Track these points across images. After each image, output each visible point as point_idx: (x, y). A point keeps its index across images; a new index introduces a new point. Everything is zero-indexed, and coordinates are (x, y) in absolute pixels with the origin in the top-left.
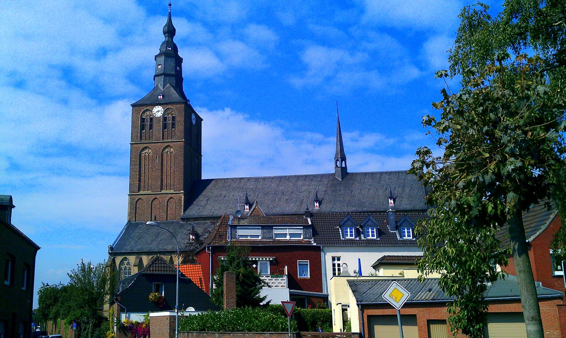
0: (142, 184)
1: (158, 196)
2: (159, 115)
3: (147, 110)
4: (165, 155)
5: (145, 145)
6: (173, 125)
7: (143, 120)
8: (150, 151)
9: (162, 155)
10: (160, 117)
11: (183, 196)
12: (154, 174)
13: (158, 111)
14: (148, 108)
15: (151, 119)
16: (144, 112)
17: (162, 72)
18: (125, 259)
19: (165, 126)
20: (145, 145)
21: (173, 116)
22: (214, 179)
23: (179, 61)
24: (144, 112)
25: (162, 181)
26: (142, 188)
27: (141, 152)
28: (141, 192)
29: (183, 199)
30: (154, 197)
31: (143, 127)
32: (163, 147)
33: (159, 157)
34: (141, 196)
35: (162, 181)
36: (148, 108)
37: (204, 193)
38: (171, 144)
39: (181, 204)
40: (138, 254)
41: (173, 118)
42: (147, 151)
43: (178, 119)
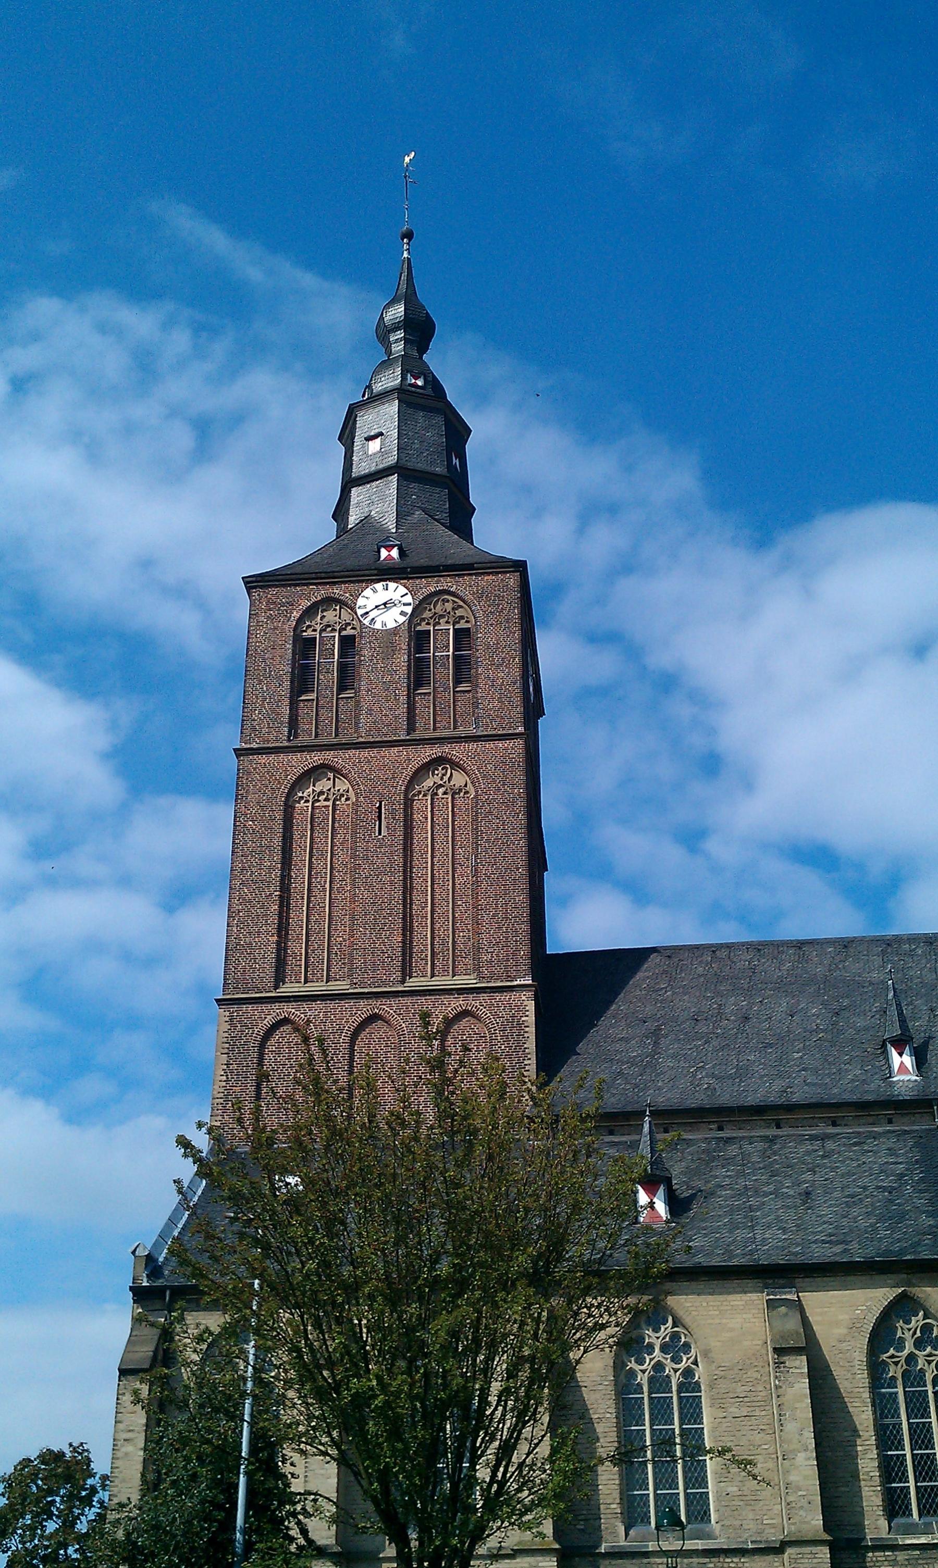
0: (297, 947)
1: (386, 1007)
2: (392, 619)
3: (329, 601)
4: (423, 805)
5: (316, 758)
6: (463, 668)
7: (304, 647)
8: (342, 785)
9: (408, 804)
10: (395, 631)
11: (531, 1006)
12: (363, 893)
13: (384, 606)
14: (337, 591)
15: (348, 643)
16: (310, 612)
17: (392, 459)
18: (655, 1315)
19: (419, 674)
20: (316, 758)
21: (462, 625)
22: (654, 950)
23: (457, 433)
24: (310, 612)
25: (407, 929)
26: (295, 964)
27: (289, 795)
28: (289, 988)
29: (531, 1019)
30: (365, 1008)
31: (302, 680)
32: (410, 770)
33: (393, 812)
34: (289, 1010)
35: (407, 929)
36: (337, 591)
37: (620, 1006)
38: (455, 751)
39: (520, 1045)
40: (777, 1276)
41: (463, 637)
42: (323, 785)
43: (485, 637)
